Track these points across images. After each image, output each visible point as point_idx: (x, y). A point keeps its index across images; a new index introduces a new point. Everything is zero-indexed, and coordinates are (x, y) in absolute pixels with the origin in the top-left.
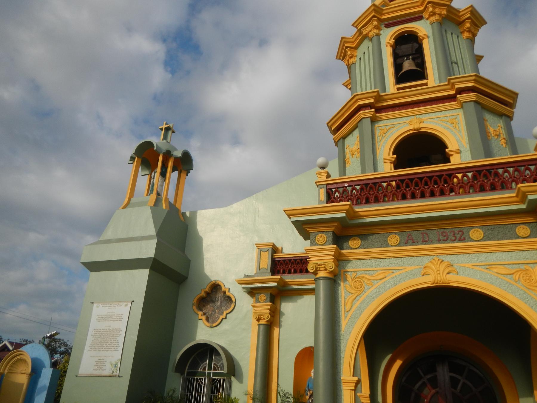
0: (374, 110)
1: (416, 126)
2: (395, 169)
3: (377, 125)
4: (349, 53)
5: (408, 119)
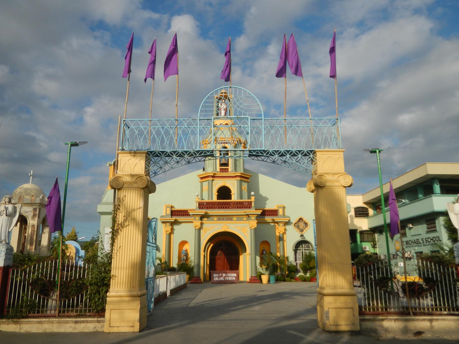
0: (213, 178)
1: (224, 184)
2: (217, 200)
3: (213, 182)
4: (205, 145)
5: (222, 181)
